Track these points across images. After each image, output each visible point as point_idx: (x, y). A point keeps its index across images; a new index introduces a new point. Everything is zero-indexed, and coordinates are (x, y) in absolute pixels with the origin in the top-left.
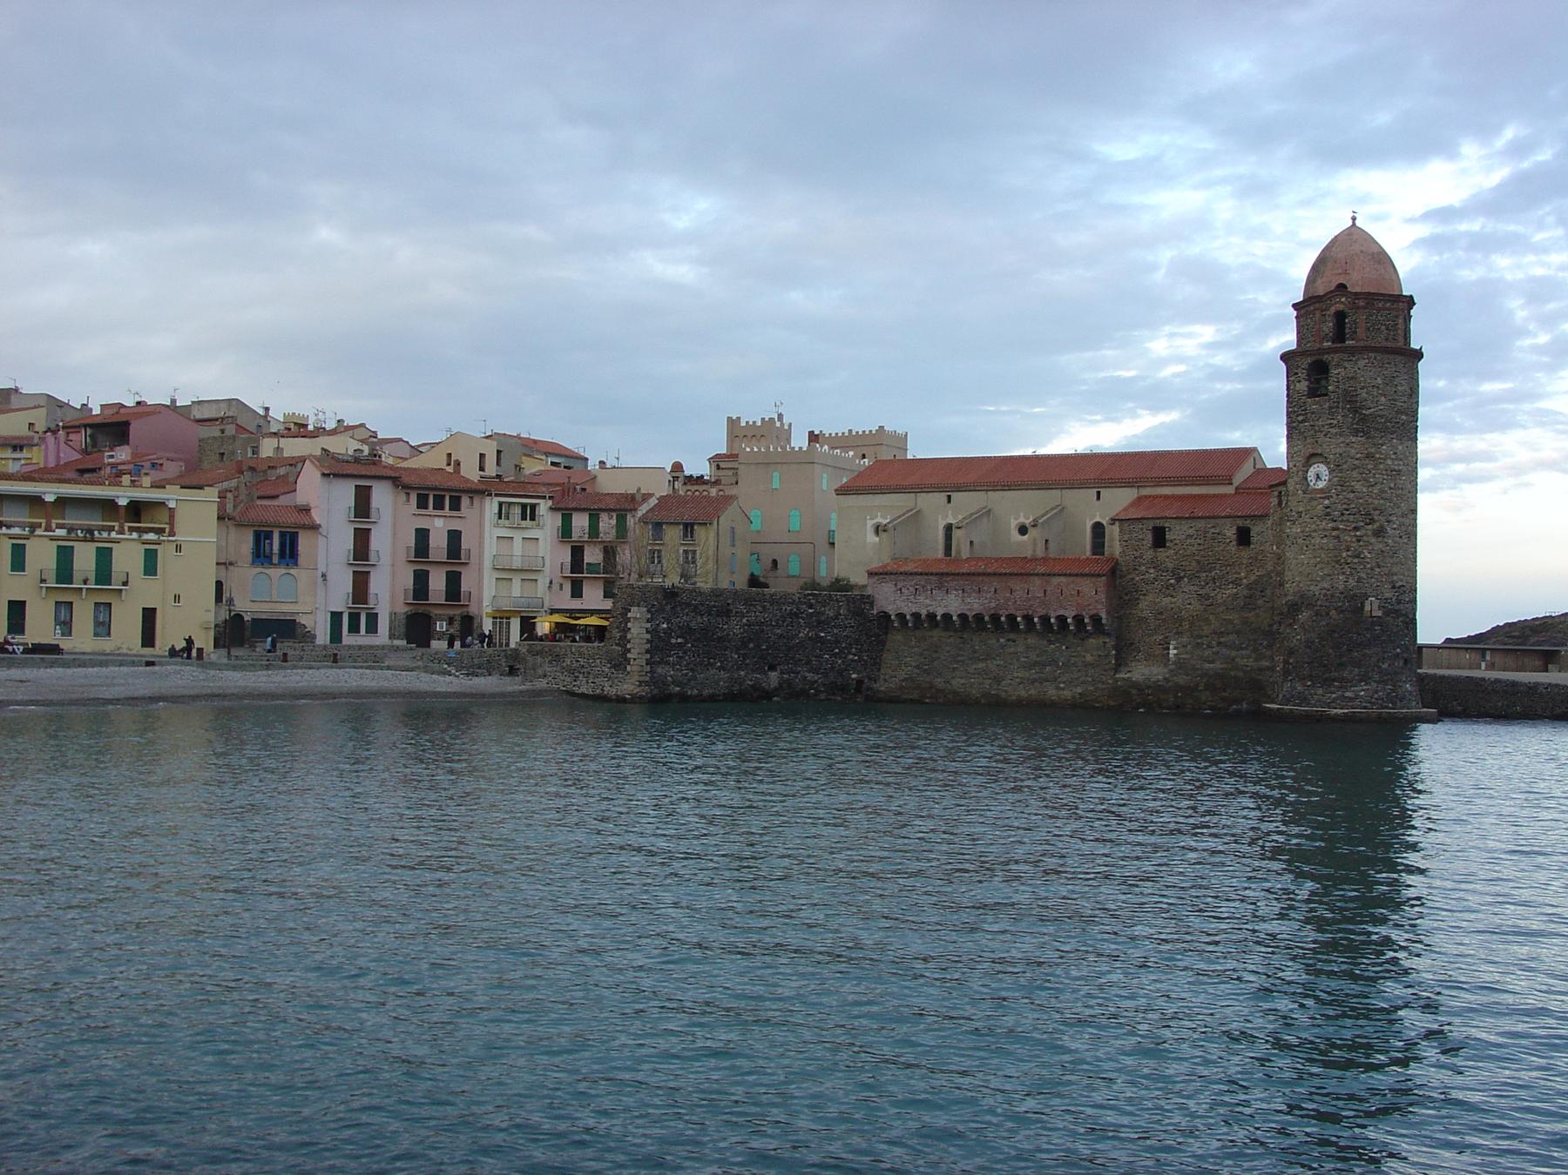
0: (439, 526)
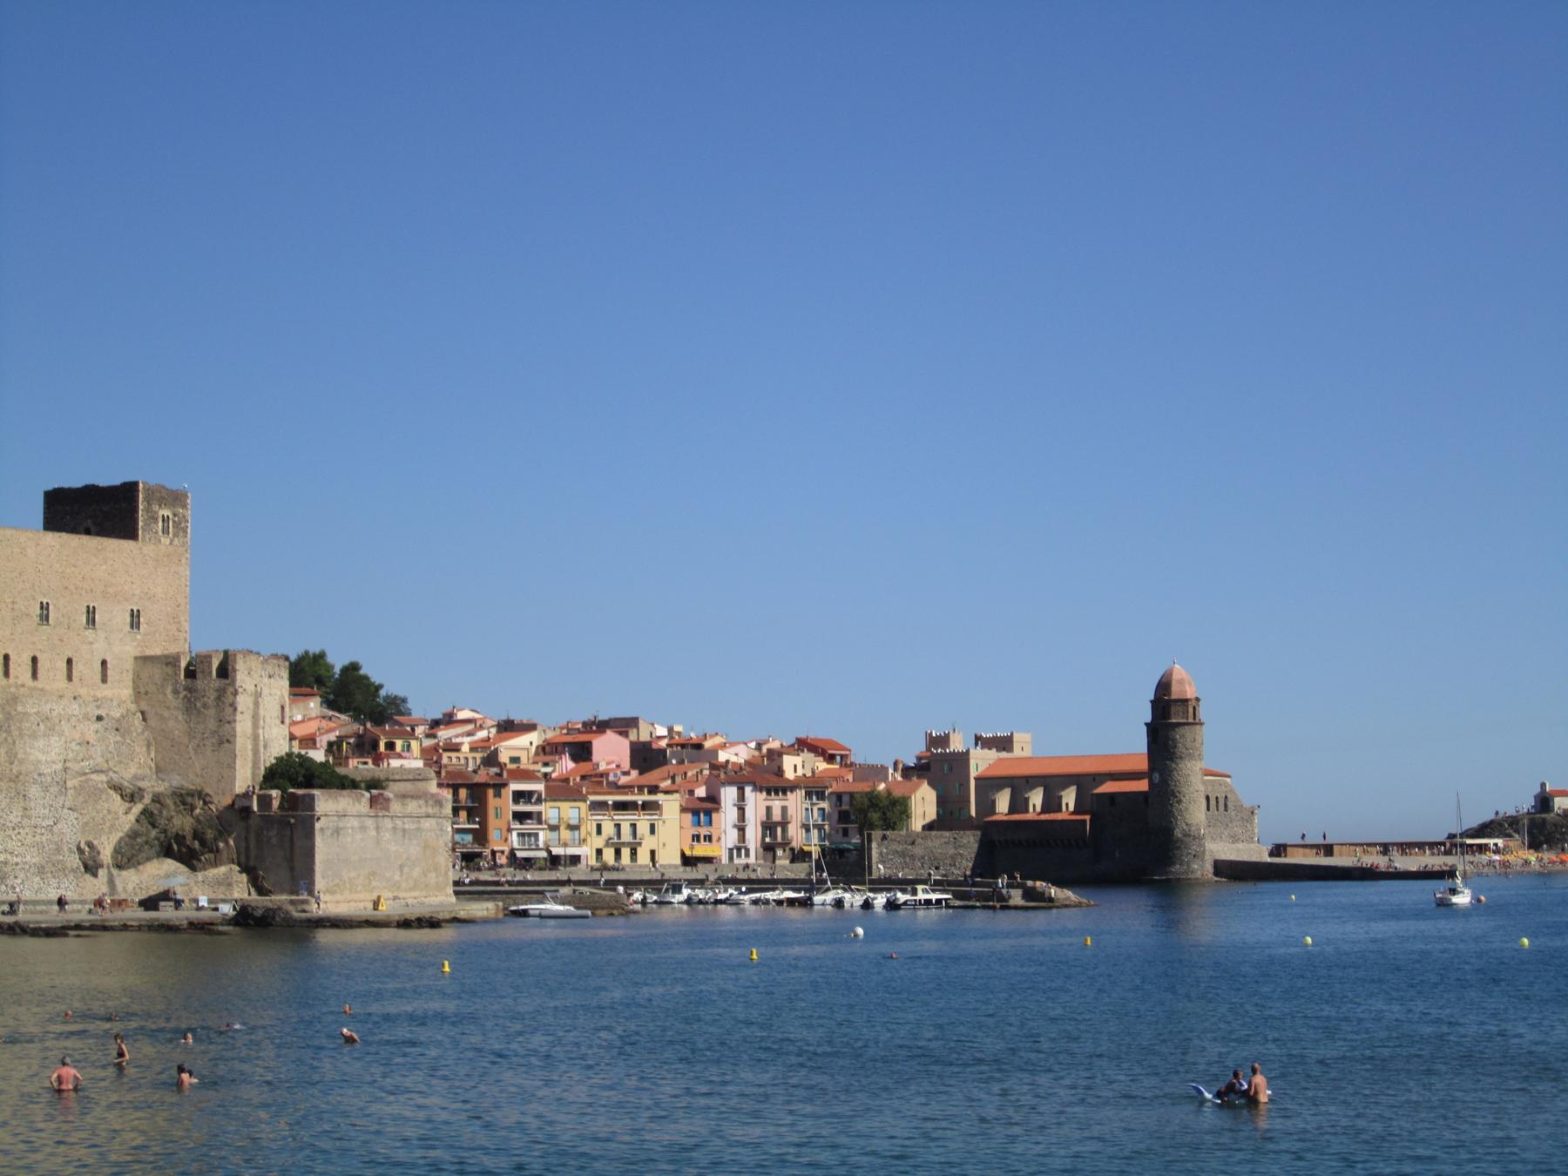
0: (776, 804)
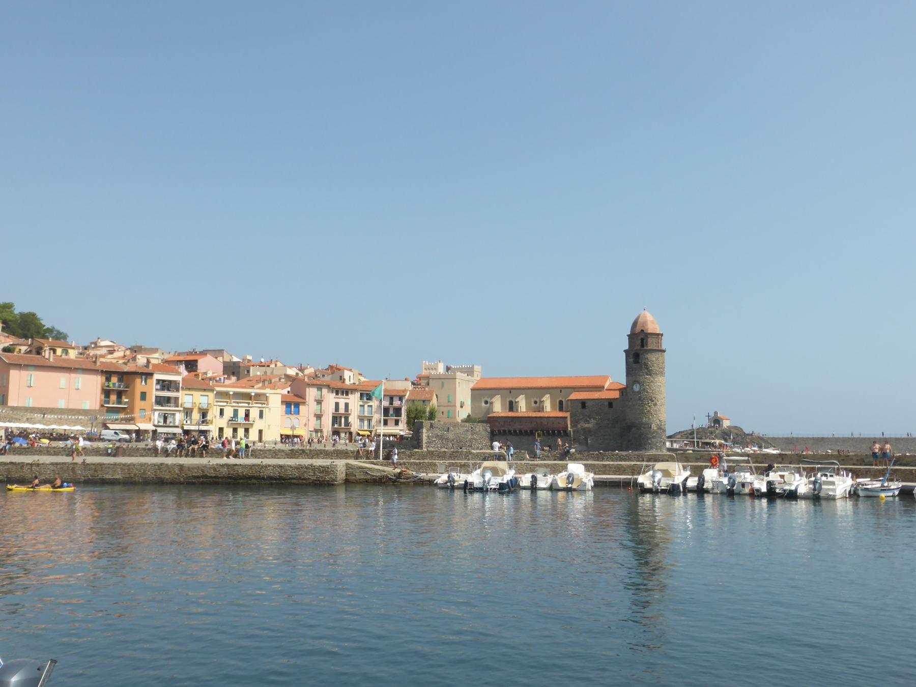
0: (342, 402)
